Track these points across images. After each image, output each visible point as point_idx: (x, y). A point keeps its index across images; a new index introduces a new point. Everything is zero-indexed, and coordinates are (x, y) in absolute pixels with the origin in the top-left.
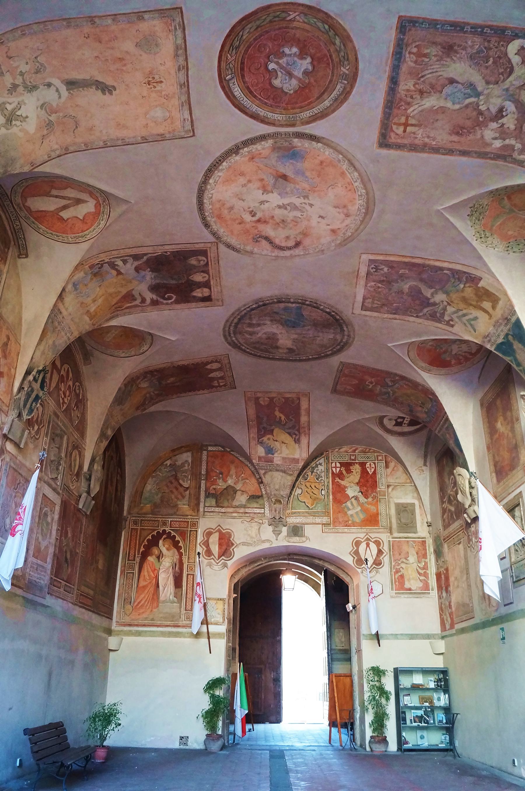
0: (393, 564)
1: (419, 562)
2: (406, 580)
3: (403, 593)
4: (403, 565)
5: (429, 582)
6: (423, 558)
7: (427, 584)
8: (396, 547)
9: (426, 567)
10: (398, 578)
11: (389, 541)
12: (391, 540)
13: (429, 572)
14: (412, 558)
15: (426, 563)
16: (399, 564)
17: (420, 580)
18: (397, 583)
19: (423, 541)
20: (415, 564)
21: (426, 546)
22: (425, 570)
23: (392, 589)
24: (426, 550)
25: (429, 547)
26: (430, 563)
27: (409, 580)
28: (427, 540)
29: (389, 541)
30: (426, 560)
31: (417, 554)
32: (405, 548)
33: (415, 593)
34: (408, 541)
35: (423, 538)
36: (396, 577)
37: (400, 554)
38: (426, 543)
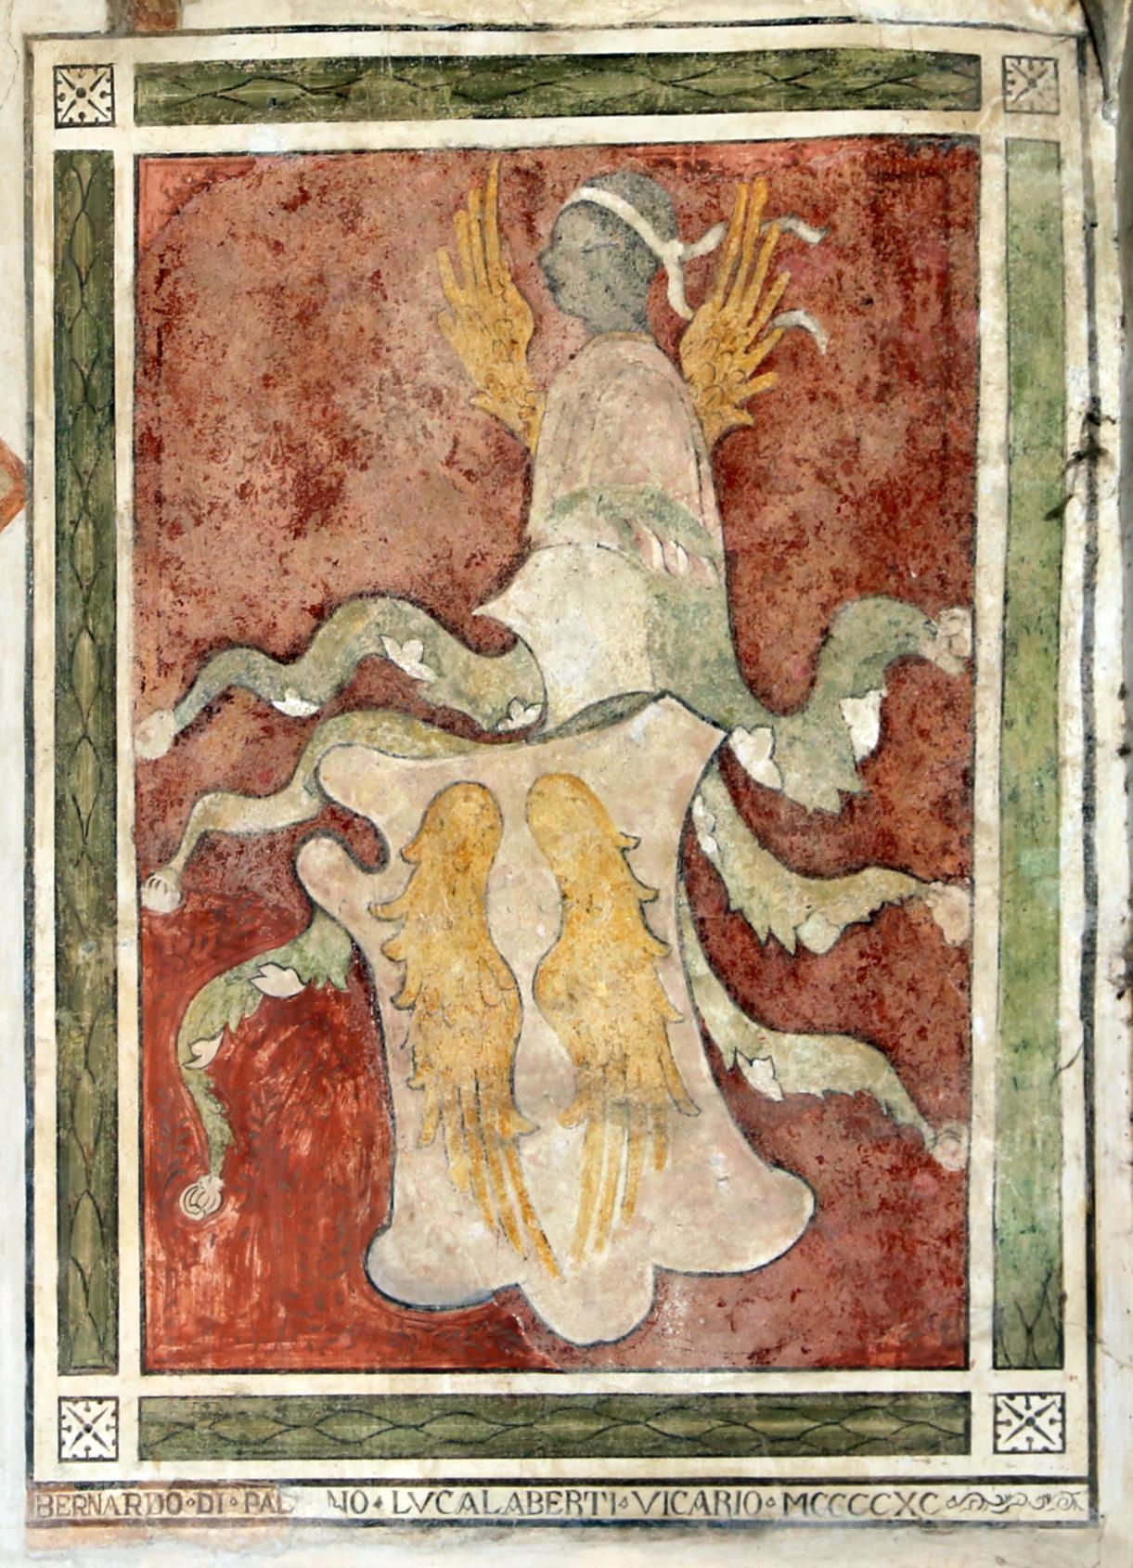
0: (145, 735)
1: (769, 687)
2: (408, 1107)
3: (324, 1430)
4: (375, 772)
5: (978, 1151)
6: (880, 577)
7: (901, 1210)
8: (231, 339)
9: (913, 797)
10: (231, 1080)
11: (84, 182)
12: (126, 142)
13: (972, 914)
14: (594, 610)
15: (925, 706)
16: (279, 745)
17: (762, 1127)
18: (205, 1194)
19: (894, 163)
20: (668, 741)
21: (954, 295)
22: (878, 885)
23: (86, 1340)
24: (956, 372)
25: (1038, 325)
26: (1032, 707)
27: (490, 1118)
28: (991, 129)
29: (84, 182)
30: (943, 641)
31: (733, 471)
32: (445, 331)
33: (610, 1425)
34: (530, 177)
35: (902, 79)
36: (200, 1048)
37: (317, 502)
38: (957, 215)
